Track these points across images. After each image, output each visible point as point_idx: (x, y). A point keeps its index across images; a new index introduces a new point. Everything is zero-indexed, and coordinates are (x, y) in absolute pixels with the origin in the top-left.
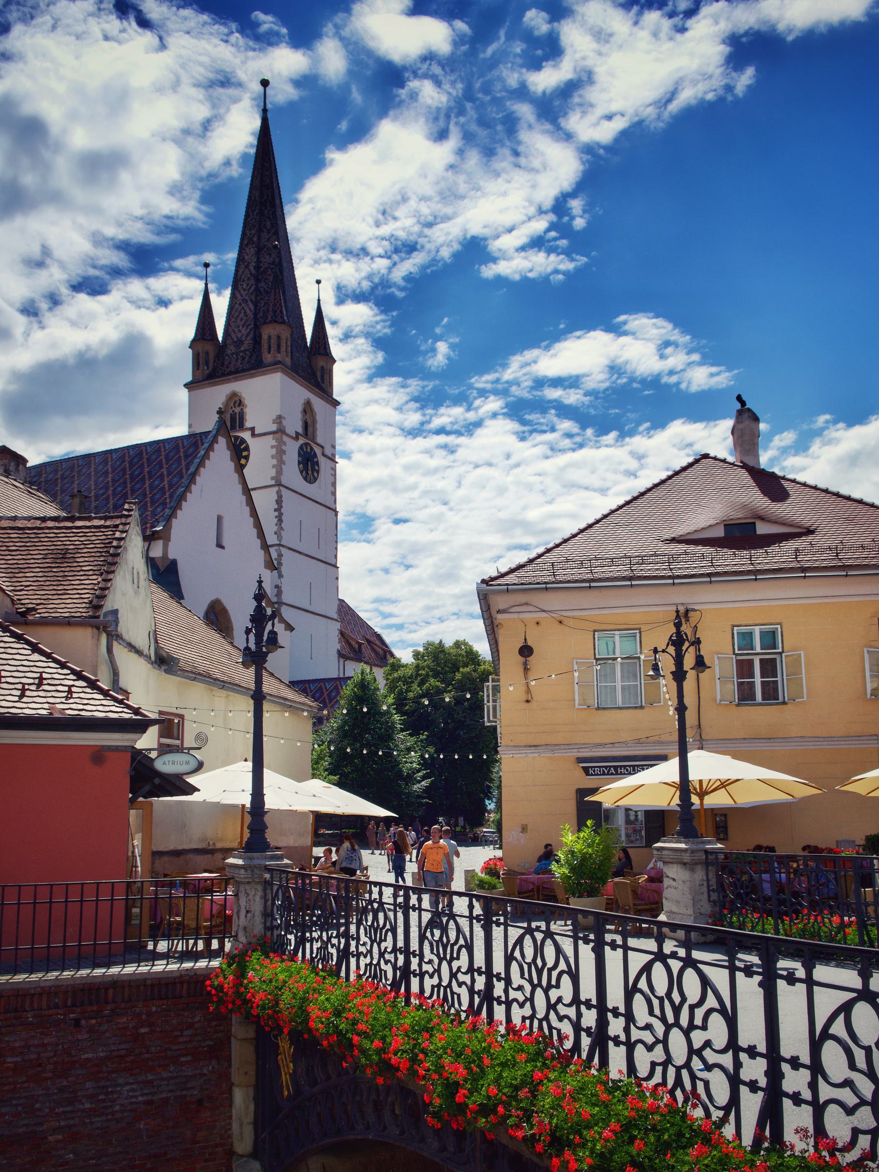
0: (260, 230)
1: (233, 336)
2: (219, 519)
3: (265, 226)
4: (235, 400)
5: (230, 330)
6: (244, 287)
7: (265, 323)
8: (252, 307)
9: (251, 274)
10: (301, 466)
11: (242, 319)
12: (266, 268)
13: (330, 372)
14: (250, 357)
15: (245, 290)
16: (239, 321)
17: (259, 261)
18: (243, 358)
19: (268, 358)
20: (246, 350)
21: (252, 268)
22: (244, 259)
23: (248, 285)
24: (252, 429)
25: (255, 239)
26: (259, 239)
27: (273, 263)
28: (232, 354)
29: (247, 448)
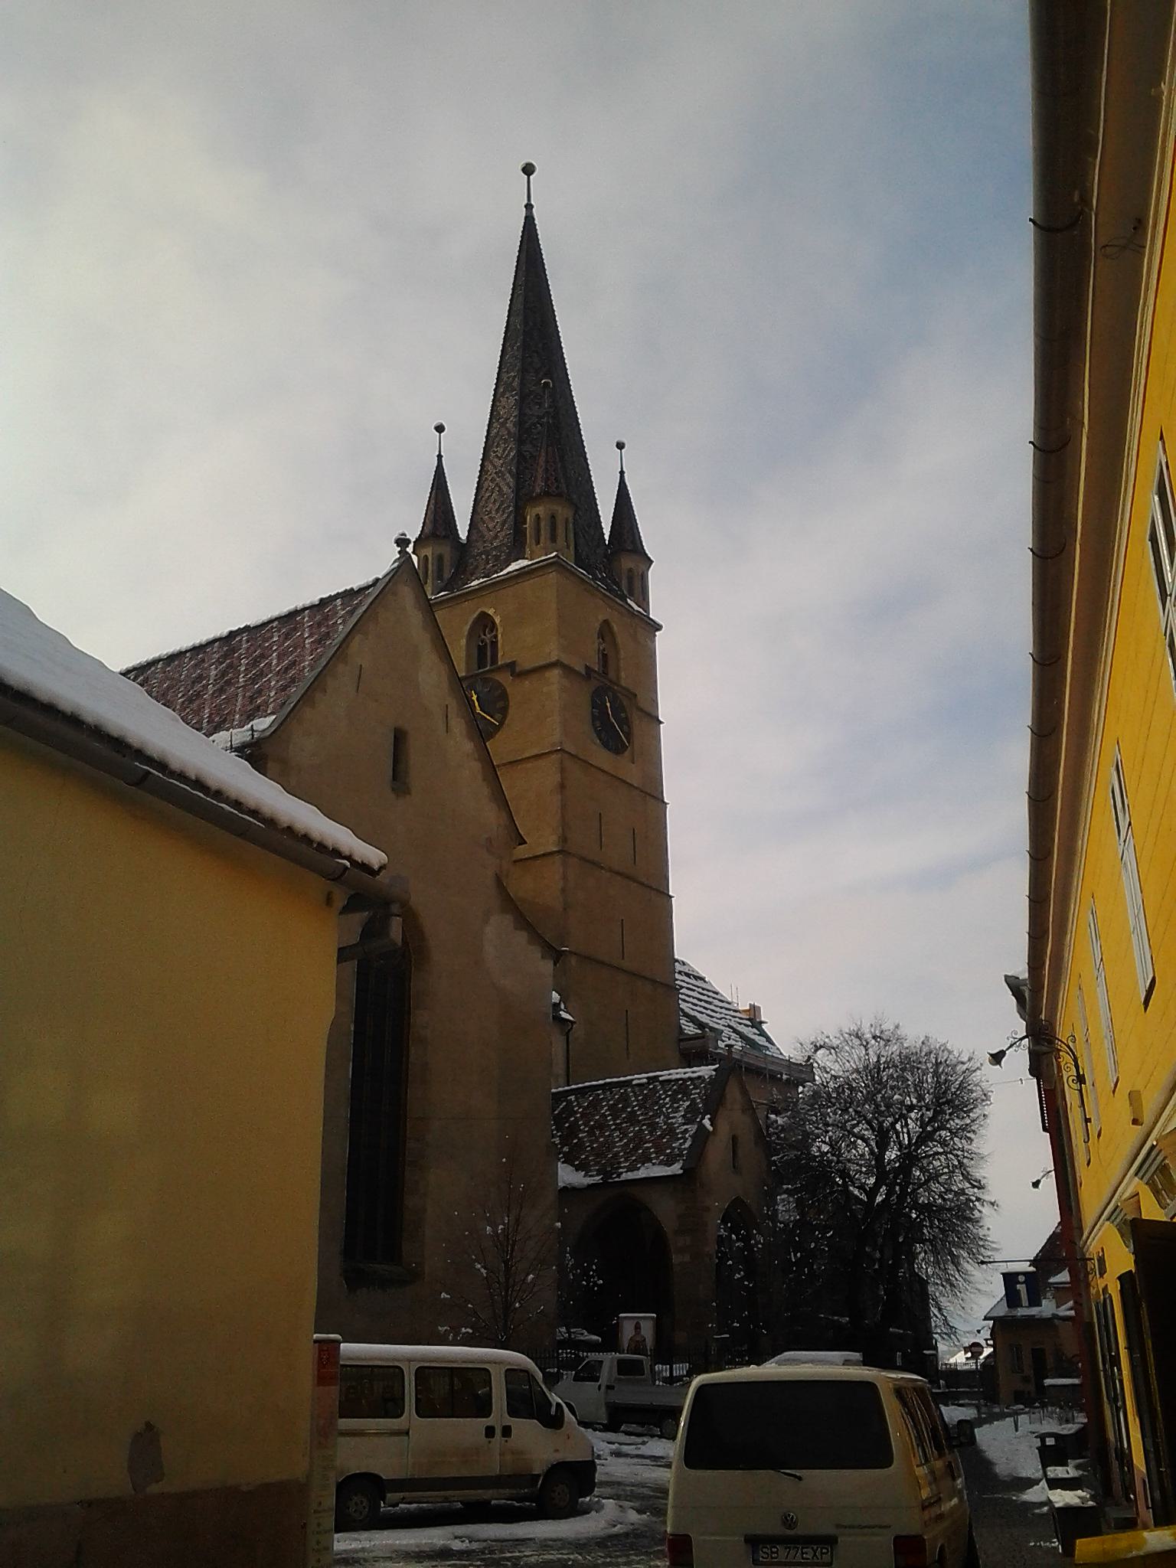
1: (483, 528)
2: (399, 738)
4: (484, 622)
9: (509, 432)
10: (598, 724)
11: (494, 502)
13: (644, 578)
17: (521, 414)
24: (511, 666)
25: (515, 384)
26: (522, 384)
29: (504, 696)
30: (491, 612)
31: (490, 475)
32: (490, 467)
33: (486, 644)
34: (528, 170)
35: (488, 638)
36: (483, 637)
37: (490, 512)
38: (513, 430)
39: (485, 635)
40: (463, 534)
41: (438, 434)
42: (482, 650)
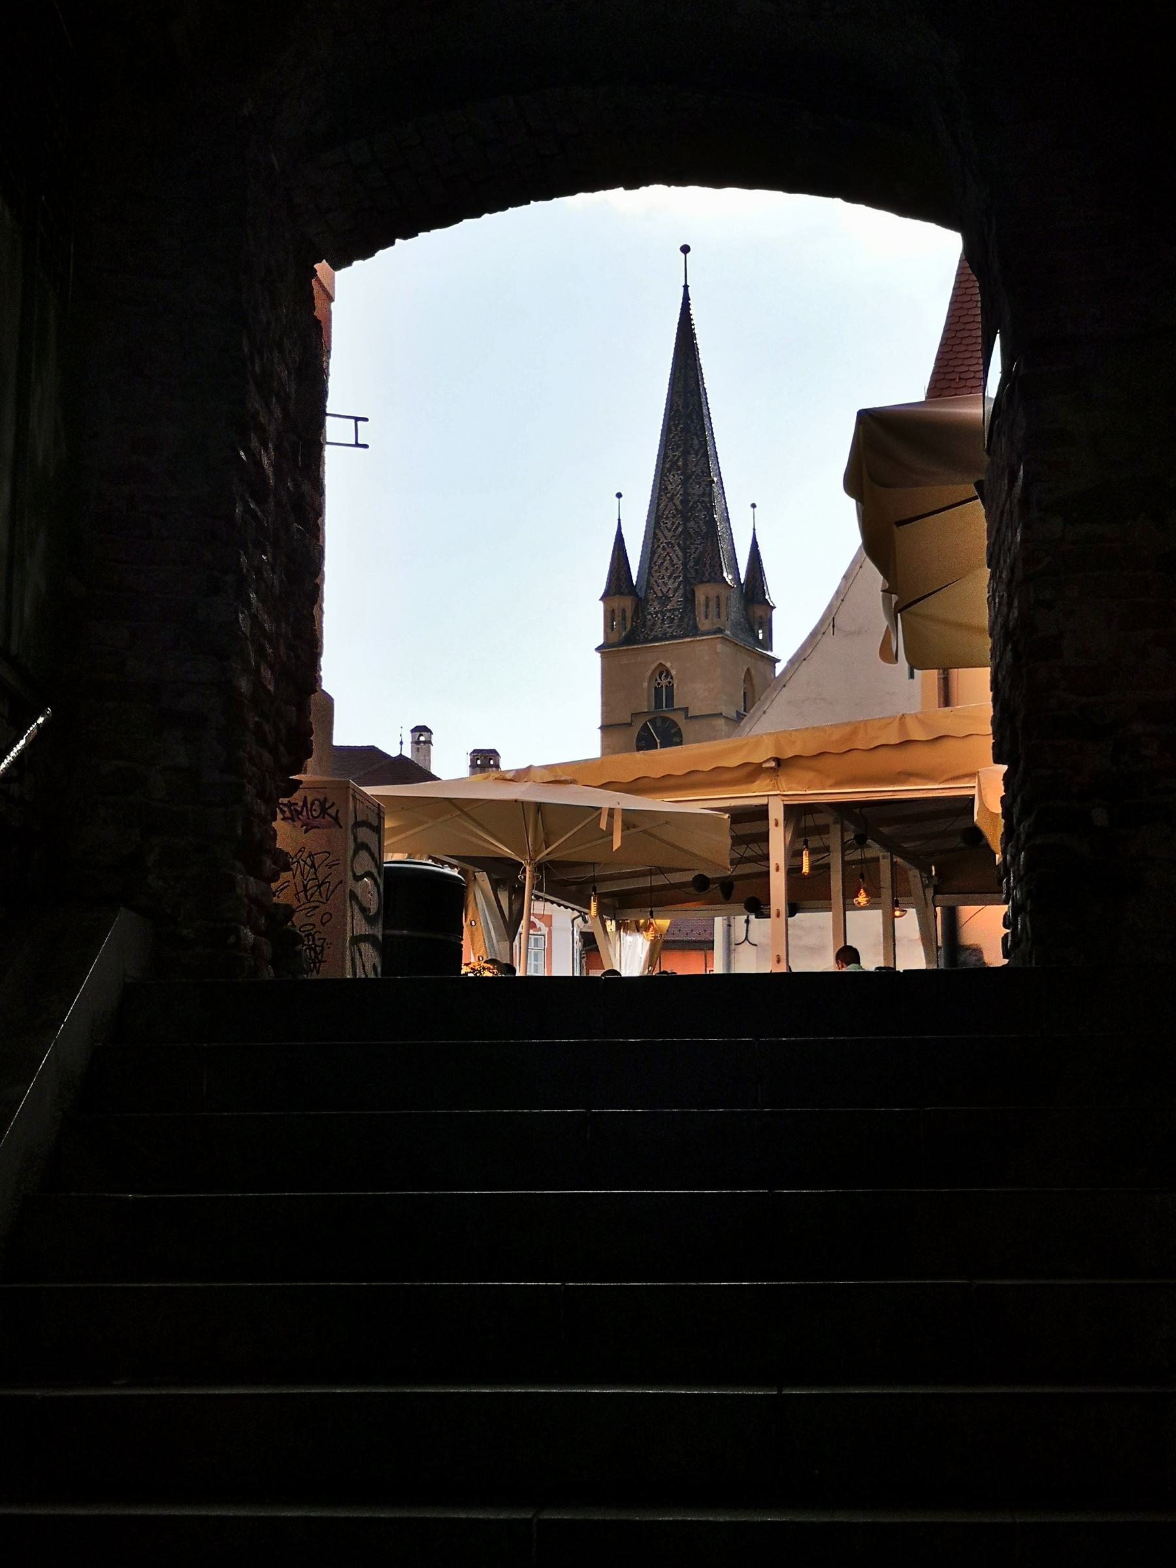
0: (686, 453)
1: (657, 589)
3: (691, 446)
4: (663, 671)
5: (652, 581)
6: (669, 525)
7: (702, 582)
8: (680, 554)
9: (676, 509)
11: (667, 569)
12: (695, 503)
14: (681, 619)
15: (669, 530)
16: (663, 571)
18: (672, 620)
19: (704, 624)
20: (674, 610)
21: (678, 503)
22: (666, 488)
23: (673, 523)
25: (680, 463)
27: (703, 495)
28: (656, 613)
30: (668, 665)
31: (662, 543)
32: (660, 535)
33: (662, 686)
34: (685, 249)
35: (664, 682)
36: (659, 681)
37: (663, 578)
38: (680, 507)
39: (660, 679)
40: (635, 584)
41: (618, 499)
42: (658, 691)
